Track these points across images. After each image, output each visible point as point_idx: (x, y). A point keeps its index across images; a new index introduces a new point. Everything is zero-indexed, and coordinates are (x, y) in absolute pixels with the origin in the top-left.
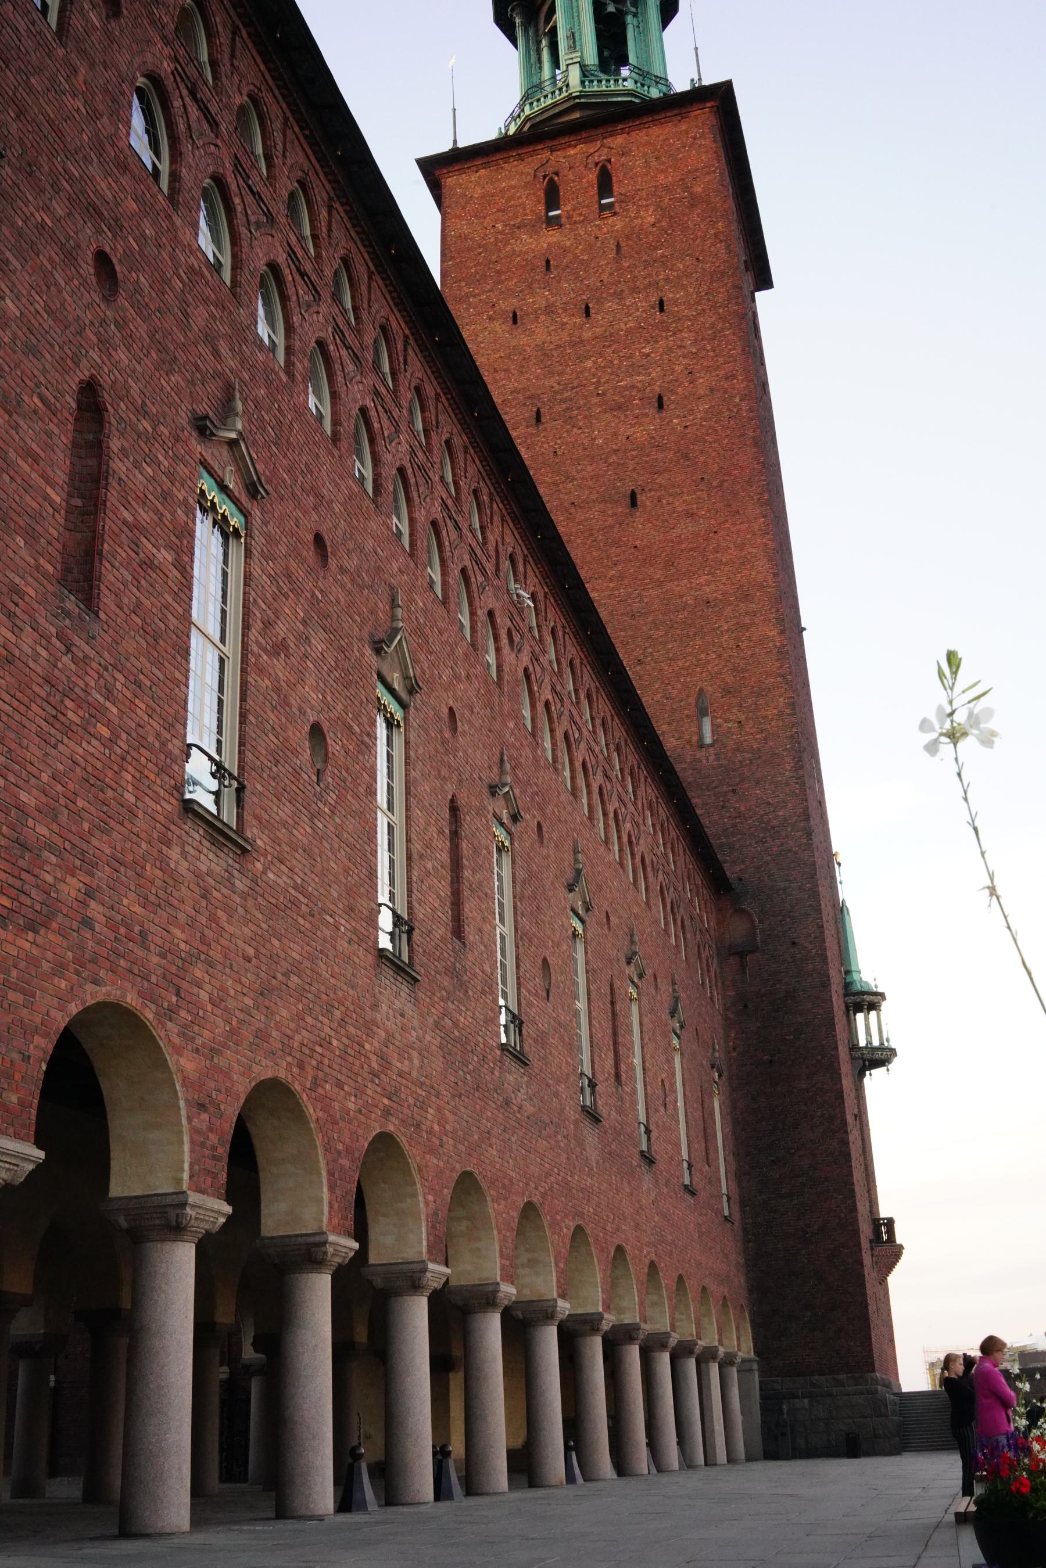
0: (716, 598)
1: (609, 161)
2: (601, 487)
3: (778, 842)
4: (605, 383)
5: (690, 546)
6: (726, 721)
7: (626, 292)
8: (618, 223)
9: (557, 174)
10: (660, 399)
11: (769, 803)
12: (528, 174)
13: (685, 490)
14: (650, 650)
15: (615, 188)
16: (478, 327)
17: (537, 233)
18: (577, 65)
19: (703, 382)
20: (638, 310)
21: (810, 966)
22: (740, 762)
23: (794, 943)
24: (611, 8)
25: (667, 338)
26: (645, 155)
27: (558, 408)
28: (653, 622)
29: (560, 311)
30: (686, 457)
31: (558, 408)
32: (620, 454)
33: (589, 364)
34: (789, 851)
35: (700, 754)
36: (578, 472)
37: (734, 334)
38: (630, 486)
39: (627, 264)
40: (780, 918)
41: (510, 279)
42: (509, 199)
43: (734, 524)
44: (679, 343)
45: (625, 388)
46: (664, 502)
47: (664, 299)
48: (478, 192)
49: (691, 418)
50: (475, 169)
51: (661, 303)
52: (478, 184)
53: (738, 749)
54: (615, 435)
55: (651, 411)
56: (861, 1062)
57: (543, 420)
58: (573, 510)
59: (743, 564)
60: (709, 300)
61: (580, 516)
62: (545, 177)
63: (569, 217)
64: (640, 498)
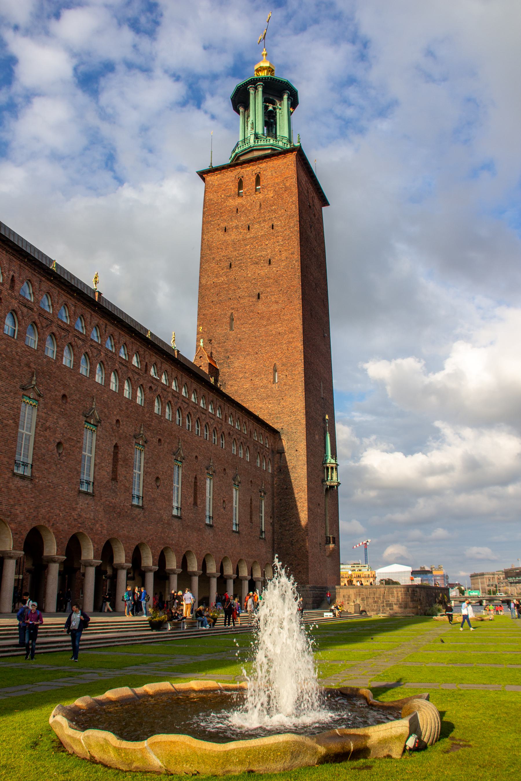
0: (282, 332)
1: (260, 173)
2: (249, 291)
4: (253, 254)
5: (275, 313)
6: (282, 375)
7: (262, 222)
8: (261, 196)
9: (243, 177)
10: (270, 260)
11: (293, 403)
12: (233, 177)
15: (261, 183)
16: (214, 233)
17: (234, 199)
18: (254, 135)
19: (284, 255)
20: (265, 228)
21: (301, 458)
23: (297, 450)
24: (270, 108)
25: (273, 239)
26: (272, 171)
27: (237, 263)
28: (262, 339)
29: (240, 228)
30: (276, 282)
31: (237, 263)
32: (256, 280)
33: (248, 247)
35: (274, 386)
36: (242, 286)
37: (295, 238)
38: (258, 291)
39: (263, 211)
41: (225, 215)
42: (227, 186)
43: (290, 306)
45: (259, 256)
48: (216, 183)
51: (273, 226)
52: (217, 180)
53: (285, 384)
54: (254, 273)
55: (267, 265)
57: (232, 267)
58: (239, 299)
59: (292, 320)
60: (288, 226)
61: (242, 302)
62: (239, 178)
63: (245, 193)
64: (261, 296)
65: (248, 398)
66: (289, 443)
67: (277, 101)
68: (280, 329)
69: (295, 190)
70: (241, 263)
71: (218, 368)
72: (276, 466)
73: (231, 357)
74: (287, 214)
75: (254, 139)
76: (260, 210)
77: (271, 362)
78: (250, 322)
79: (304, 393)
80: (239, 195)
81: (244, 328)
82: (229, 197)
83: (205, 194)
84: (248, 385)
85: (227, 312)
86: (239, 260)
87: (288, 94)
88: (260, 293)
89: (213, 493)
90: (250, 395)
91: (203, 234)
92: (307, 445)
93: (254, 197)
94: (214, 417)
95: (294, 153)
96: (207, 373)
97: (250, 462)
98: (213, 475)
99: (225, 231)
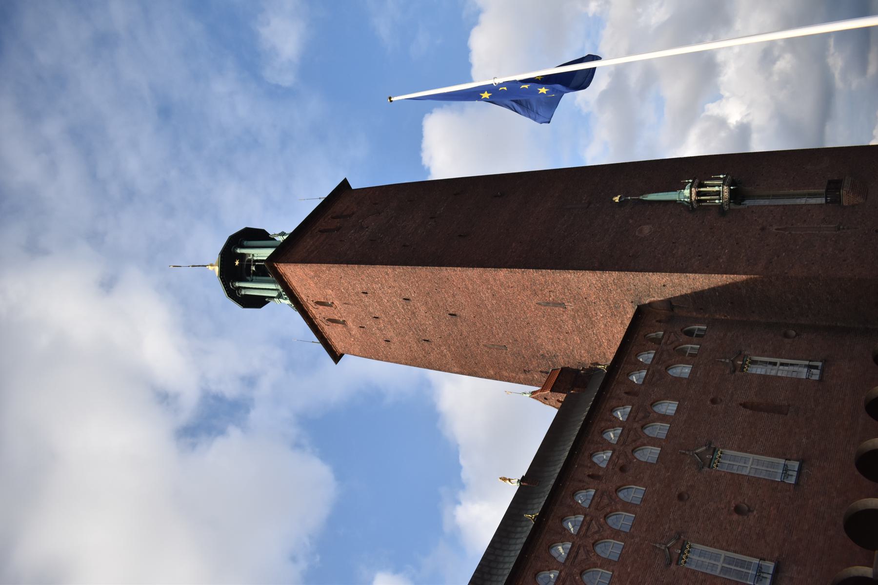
3: (610, 285)
8: (336, 302)
9: (324, 318)
10: (404, 299)
11: (590, 286)
13: (443, 296)
22: (570, 294)
23: (664, 286)
24: (253, 268)
34: (613, 281)
39: (352, 302)
40: (651, 290)
43: (453, 281)
44: (378, 289)
45: (404, 310)
51: (363, 293)
54: (426, 316)
56: (731, 204)
61: (465, 333)
64: (451, 313)
65: (594, 339)
66: (654, 295)
67: (247, 259)
68: (487, 295)
69: (315, 266)
70: (420, 330)
71: (560, 367)
72: (695, 314)
74: (345, 276)
75: (283, 298)
76: (352, 305)
77: (536, 309)
78: (488, 327)
79: (570, 271)
82: (351, 334)
84: (575, 338)
85: (484, 351)
89: (715, 548)
90: (589, 336)
91: (401, 364)
92: (653, 272)
93: (340, 309)
94: (588, 518)
95: (276, 265)
96: (565, 395)
97: (679, 401)
98: (684, 541)
99: (389, 341)
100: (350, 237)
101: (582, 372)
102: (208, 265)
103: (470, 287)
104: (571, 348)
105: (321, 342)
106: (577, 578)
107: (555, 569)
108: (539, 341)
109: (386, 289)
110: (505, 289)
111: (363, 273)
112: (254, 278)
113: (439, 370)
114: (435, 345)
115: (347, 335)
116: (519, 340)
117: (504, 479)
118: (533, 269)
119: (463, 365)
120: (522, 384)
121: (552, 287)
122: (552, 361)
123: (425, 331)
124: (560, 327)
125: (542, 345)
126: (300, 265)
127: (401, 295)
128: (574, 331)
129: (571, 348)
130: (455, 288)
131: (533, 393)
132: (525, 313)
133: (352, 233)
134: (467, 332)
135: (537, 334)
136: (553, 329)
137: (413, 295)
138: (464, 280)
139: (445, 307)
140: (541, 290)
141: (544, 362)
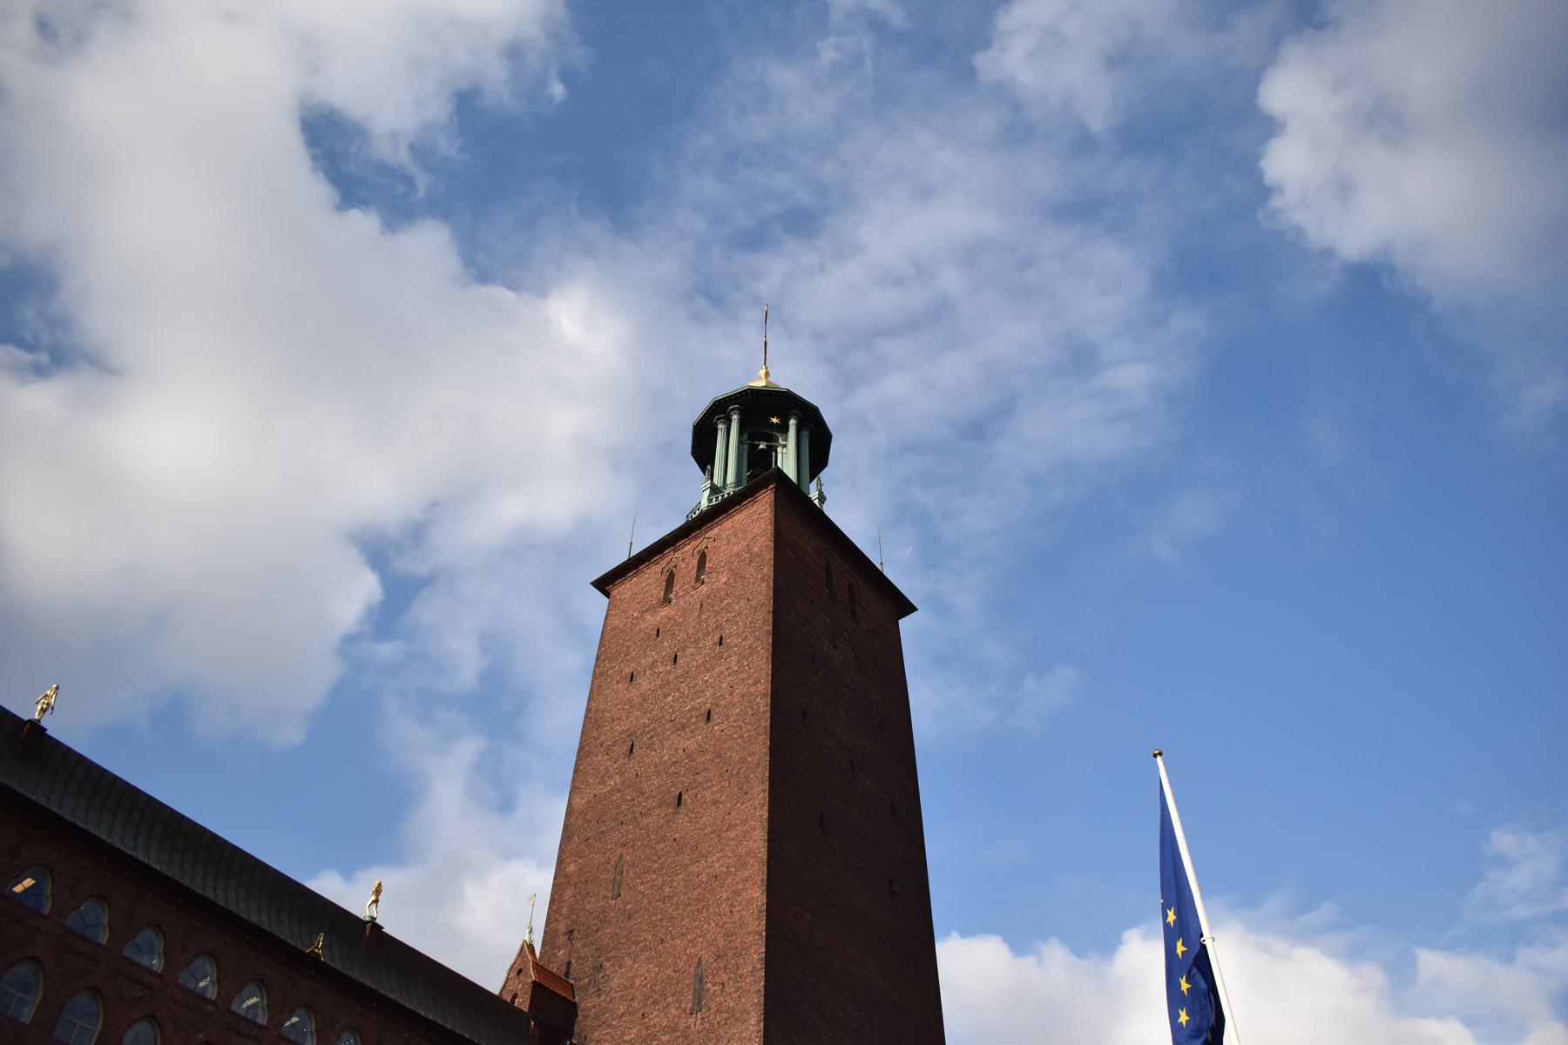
1: (707, 547)
6: (714, 985)
8: (704, 589)
9: (675, 567)
10: (709, 712)
14: (670, 929)
22: (718, 1023)
33: (670, 698)
35: (692, 1020)
39: (704, 617)
45: (689, 711)
46: (699, 796)
47: (723, 635)
49: (726, 722)
50: (629, 579)
51: (721, 638)
57: (634, 751)
61: (644, 821)
64: (684, 797)
67: (777, 434)
68: (717, 865)
69: (769, 556)
70: (652, 737)
71: (577, 1000)
73: (607, 965)
75: (710, 495)
77: (690, 957)
78: (656, 866)
79: (762, 1025)
80: (666, 601)
81: (642, 883)
83: (605, 621)
84: (634, 1031)
86: (649, 733)
87: (798, 416)
88: (683, 792)
91: (589, 701)
95: (771, 486)
96: (526, 1010)
99: (631, 680)
100: (819, 617)
101: (568, 1043)
102: (766, 368)
103: (732, 834)
104: (614, 1023)
105: (630, 559)
106: (201, 1035)
107: (219, 993)
108: (628, 961)
109: (729, 679)
110: (728, 899)
111: (757, 639)
112: (746, 447)
113: (576, 771)
114: (624, 764)
115: (645, 606)
116: (631, 923)
117: (378, 891)
118: (766, 952)
119: (585, 815)
120: (546, 926)
121: (731, 988)
122: (589, 984)
123: (650, 746)
124: (656, 1002)
125: (621, 966)
126: (771, 528)
127: (718, 705)
128: (647, 1028)
129: (614, 1023)
130: (729, 805)
131: (531, 948)
132: (682, 935)
133: (825, 622)
134: (647, 825)
135: (643, 957)
136: (651, 988)
137: (716, 728)
138: (744, 822)
139: (693, 786)
140: (725, 968)
141: (587, 970)
